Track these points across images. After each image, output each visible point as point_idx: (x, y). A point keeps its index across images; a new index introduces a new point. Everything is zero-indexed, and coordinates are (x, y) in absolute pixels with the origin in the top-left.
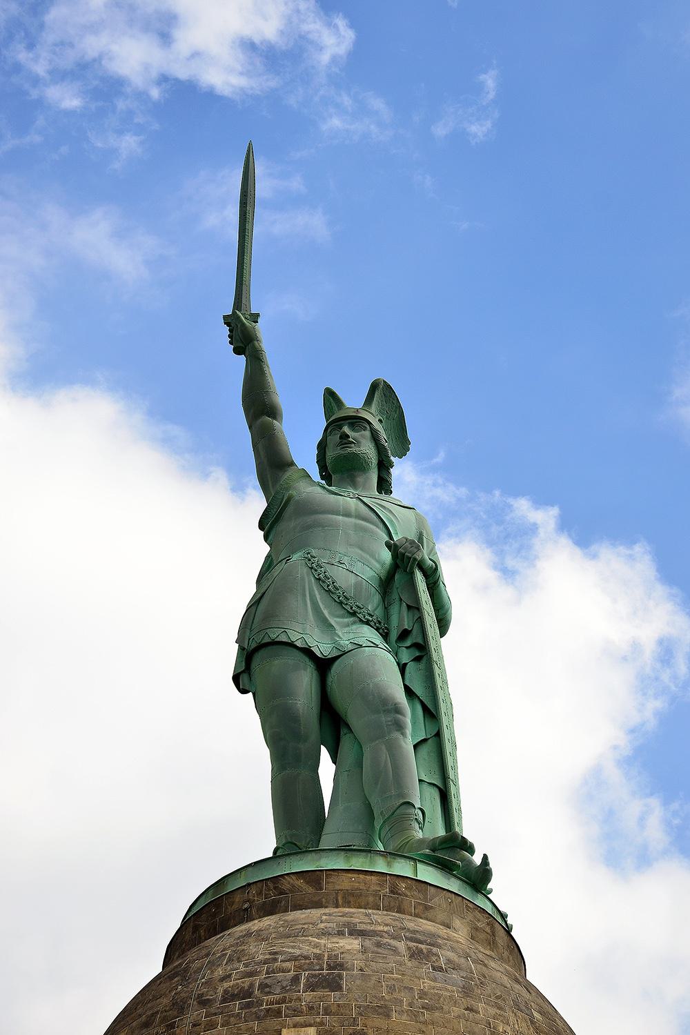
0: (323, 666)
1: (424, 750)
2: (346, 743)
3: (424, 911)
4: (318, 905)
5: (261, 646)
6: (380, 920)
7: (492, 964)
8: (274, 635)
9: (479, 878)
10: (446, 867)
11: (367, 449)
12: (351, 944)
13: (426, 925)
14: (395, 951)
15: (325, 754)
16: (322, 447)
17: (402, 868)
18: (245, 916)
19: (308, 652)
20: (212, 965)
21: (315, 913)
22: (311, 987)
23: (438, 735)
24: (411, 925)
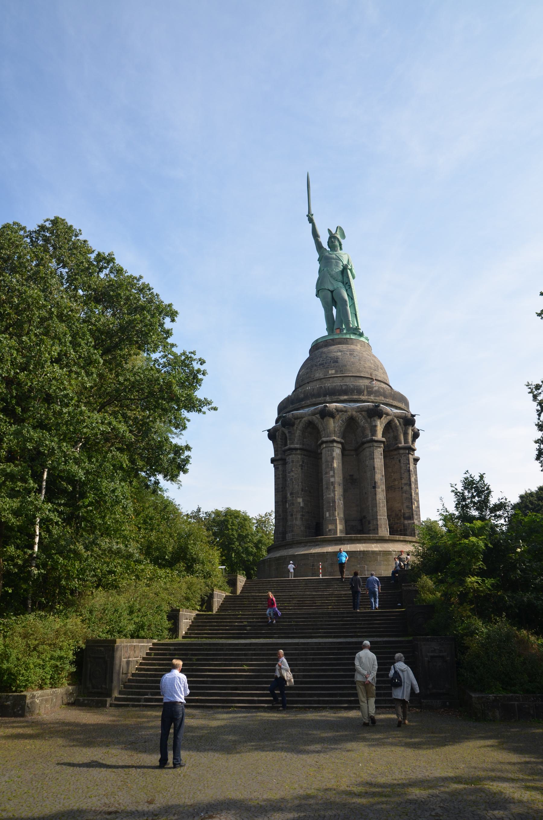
0: (332, 292)
1: (352, 307)
3: (352, 344)
4: (334, 345)
6: (344, 347)
7: (364, 353)
8: (322, 287)
9: (361, 335)
10: (355, 334)
11: (337, 243)
12: (339, 354)
13: (352, 347)
14: (347, 354)
16: (328, 242)
17: (348, 336)
18: (321, 347)
19: (329, 290)
20: (317, 358)
21: (333, 347)
22: (333, 363)
23: (354, 303)
24: (350, 348)
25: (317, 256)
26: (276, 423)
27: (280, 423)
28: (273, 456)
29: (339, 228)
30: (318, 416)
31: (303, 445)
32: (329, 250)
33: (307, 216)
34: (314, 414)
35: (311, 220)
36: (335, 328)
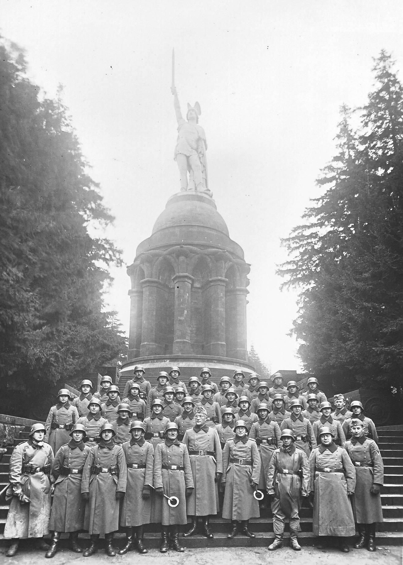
2: (191, 171)
3: (203, 201)
5: (178, 154)
9: (211, 197)
15: (188, 172)
16: (187, 115)
19: (185, 155)
23: (205, 170)
25: (176, 126)
26: (134, 262)
27: (138, 262)
28: (131, 289)
29: (197, 104)
30: (174, 255)
31: (159, 279)
32: (187, 121)
33: (171, 88)
34: (170, 254)
35: (174, 92)
36: (188, 188)
